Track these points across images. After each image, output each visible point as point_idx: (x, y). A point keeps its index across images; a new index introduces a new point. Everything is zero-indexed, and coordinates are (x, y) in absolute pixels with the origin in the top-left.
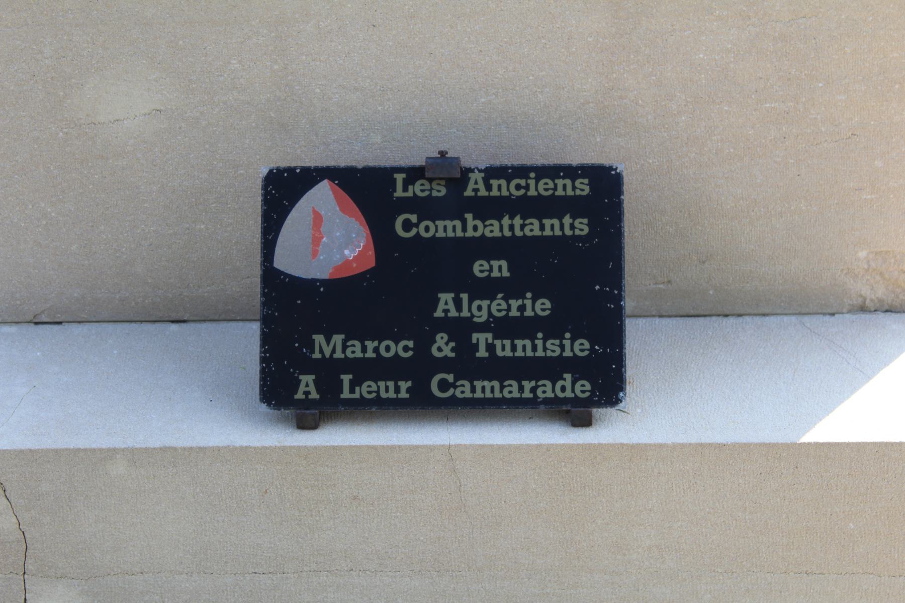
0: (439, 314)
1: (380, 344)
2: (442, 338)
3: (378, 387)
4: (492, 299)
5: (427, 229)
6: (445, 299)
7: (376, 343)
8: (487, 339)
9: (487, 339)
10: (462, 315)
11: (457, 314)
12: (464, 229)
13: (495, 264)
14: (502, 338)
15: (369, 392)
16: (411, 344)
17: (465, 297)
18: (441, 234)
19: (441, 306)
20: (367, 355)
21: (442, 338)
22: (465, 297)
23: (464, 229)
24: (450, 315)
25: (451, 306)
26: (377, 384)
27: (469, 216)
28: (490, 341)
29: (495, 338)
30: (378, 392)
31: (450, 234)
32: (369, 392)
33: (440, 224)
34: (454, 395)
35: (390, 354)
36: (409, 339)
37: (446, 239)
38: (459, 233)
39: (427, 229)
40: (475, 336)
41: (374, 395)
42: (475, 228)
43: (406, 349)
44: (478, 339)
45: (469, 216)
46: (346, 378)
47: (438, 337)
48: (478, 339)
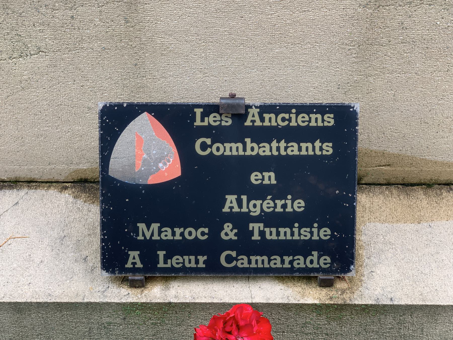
0: (226, 209)
1: (184, 230)
2: (228, 226)
3: (184, 260)
4: (264, 199)
5: (218, 149)
6: (231, 199)
7: (182, 230)
8: (259, 227)
9: (259, 227)
10: (243, 210)
11: (239, 210)
12: (245, 150)
13: (266, 174)
14: (270, 227)
15: (178, 263)
16: (206, 230)
17: (244, 198)
18: (228, 153)
19: (228, 204)
20: (175, 238)
21: (228, 226)
22: (244, 198)
23: (245, 150)
24: (234, 210)
25: (235, 204)
26: (183, 258)
27: (248, 140)
28: (262, 229)
29: (265, 227)
30: (183, 263)
31: (235, 153)
32: (178, 263)
33: (228, 145)
34: (236, 266)
35: (193, 237)
36: (205, 227)
37: (231, 157)
38: (241, 153)
39: (218, 149)
40: (251, 225)
41: (181, 265)
42: (252, 149)
43: (203, 234)
44: (253, 227)
45: (248, 140)
46: (161, 254)
47: (226, 225)
48: (253, 227)
